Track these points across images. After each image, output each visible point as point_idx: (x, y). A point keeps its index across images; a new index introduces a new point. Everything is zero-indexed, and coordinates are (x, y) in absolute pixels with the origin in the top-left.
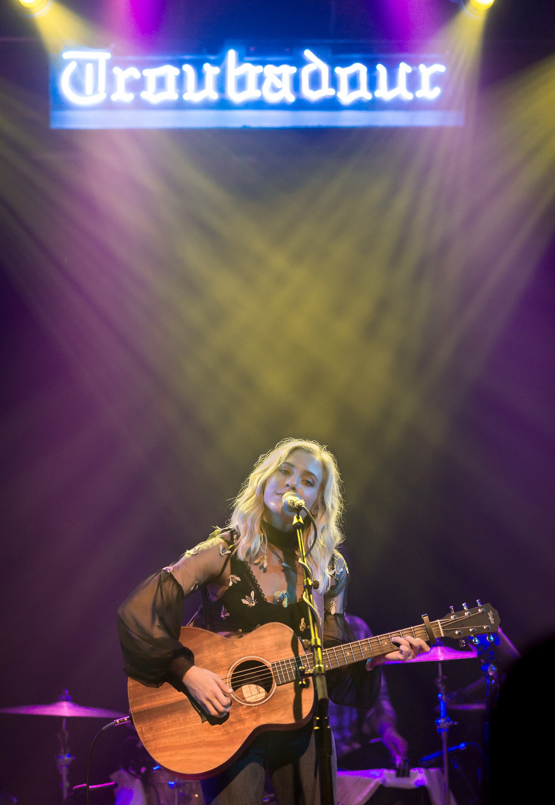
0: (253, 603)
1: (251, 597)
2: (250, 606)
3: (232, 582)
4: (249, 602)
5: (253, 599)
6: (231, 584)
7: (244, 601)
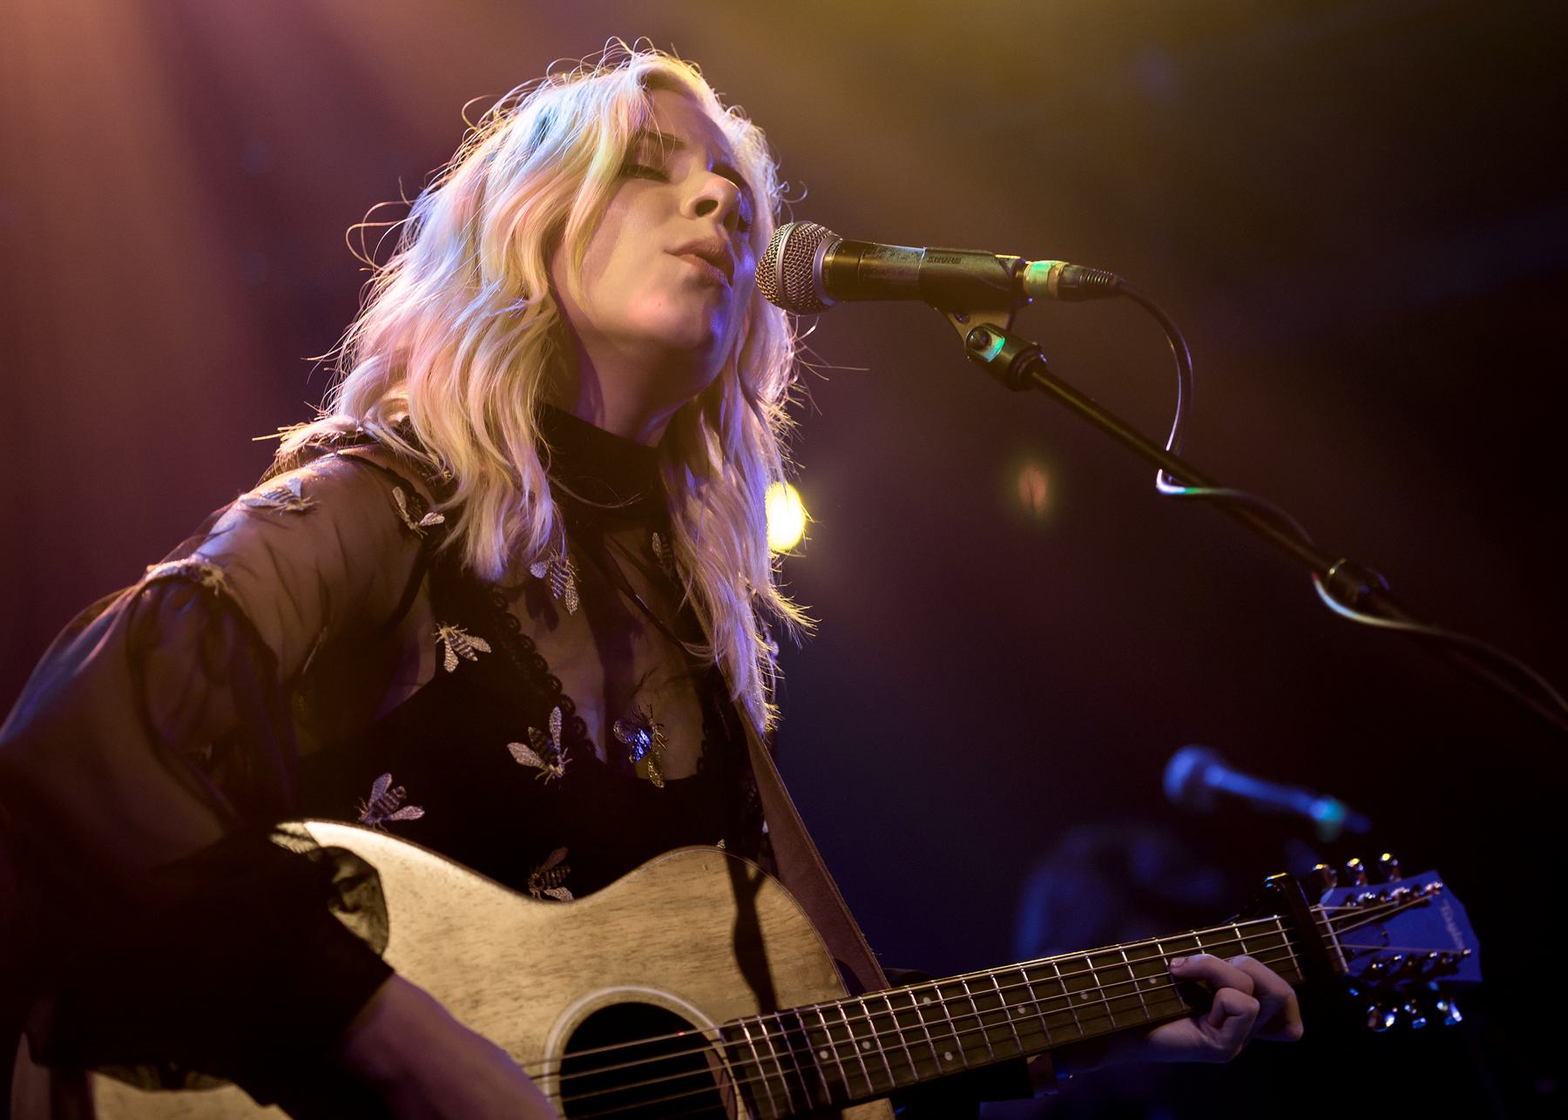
0: (556, 765)
1: (550, 736)
2: (546, 776)
3: (456, 653)
4: (542, 757)
5: (557, 745)
6: (451, 663)
7: (522, 754)
